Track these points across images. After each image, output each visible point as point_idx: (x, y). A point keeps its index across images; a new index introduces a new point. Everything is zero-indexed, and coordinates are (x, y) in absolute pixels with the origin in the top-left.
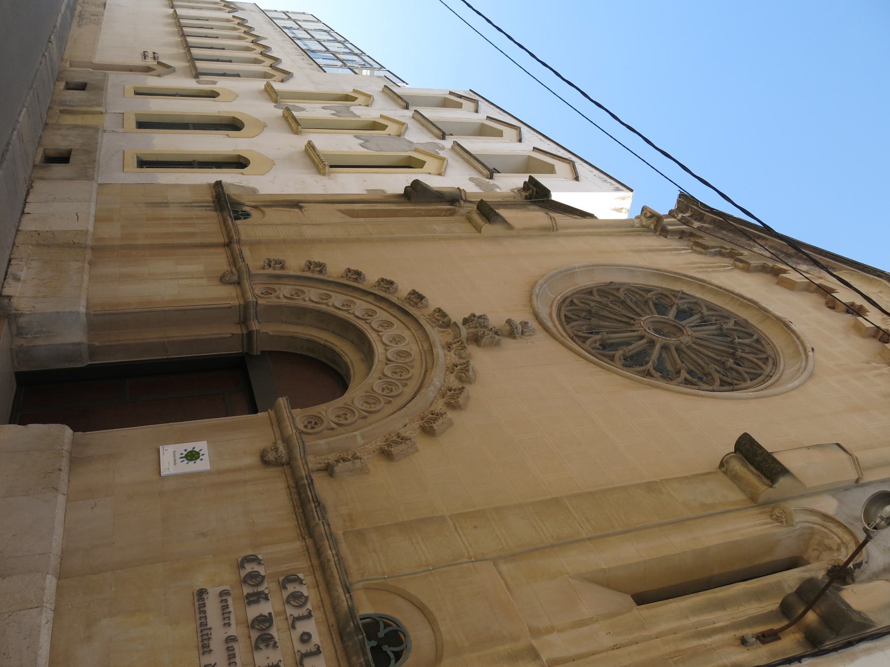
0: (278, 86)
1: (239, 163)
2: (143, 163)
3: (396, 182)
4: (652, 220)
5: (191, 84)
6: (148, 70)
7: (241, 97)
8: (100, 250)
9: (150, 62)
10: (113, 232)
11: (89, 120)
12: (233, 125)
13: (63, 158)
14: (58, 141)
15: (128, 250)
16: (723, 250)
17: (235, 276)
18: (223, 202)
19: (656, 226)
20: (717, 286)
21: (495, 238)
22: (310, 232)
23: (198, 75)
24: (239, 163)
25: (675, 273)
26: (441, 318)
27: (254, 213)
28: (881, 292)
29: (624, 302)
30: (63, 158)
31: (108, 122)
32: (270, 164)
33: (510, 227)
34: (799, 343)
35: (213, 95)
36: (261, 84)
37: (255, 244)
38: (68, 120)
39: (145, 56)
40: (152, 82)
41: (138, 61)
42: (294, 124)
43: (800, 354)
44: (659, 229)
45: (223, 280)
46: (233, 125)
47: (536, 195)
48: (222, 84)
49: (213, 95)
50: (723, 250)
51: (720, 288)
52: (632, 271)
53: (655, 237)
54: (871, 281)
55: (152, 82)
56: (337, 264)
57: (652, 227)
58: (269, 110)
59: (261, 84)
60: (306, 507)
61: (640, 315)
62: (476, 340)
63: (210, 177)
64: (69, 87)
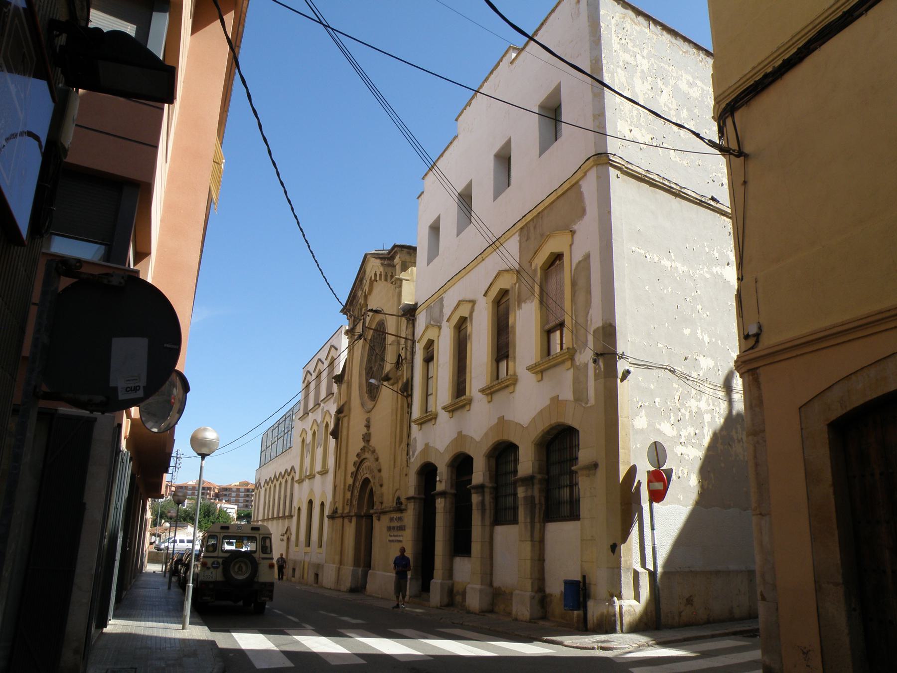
0: (297, 478)
1: (322, 504)
2: (321, 547)
3: (332, 442)
5: (295, 519)
6: (288, 539)
7: (301, 495)
8: (341, 563)
9: (285, 538)
10: (337, 558)
11: (306, 567)
12: (311, 502)
13: (317, 575)
14: (311, 578)
15: (342, 554)
17: (350, 517)
18: (331, 517)
21: (350, 410)
22: (342, 486)
23: (291, 516)
24: (322, 504)
26: (363, 449)
27: (337, 505)
30: (317, 575)
31: (307, 559)
32: (324, 493)
33: (346, 403)
35: (299, 509)
36: (296, 485)
37: (343, 508)
38: (305, 576)
39: (282, 540)
40: (293, 538)
41: (285, 543)
42: (311, 477)
45: (350, 522)
46: (311, 502)
47: (339, 379)
48: (295, 504)
49: (299, 509)
55: (293, 538)
56: (350, 481)
58: (306, 483)
59: (296, 485)
60: (384, 513)
62: (368, 441)
63: (326, 520)
64: (293, 576)
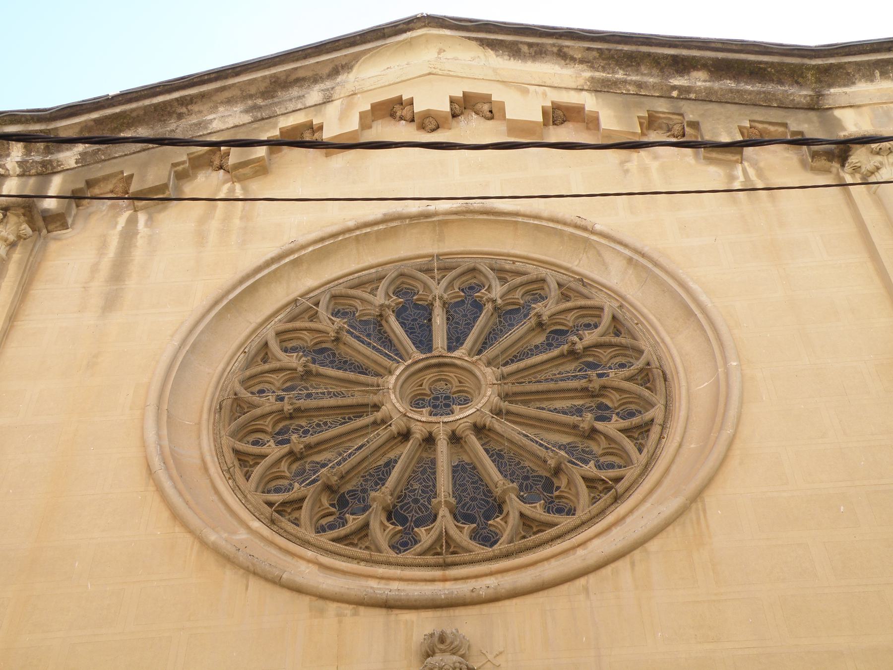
4: (12, 219)
16: (180, 168)
19: (31, 223)
20: (315, 242)
25: (241, 281)
28: (441, 51)
29: (298, 410)
34: (551, 225)
43: (586, 240)
44: (41, 223)
50: (180, 168)
51: (322, 239)
52: (194, 346)
53: (53, 246)
54: (410, 43)
57: (26, 229)
61: (376, 407)
